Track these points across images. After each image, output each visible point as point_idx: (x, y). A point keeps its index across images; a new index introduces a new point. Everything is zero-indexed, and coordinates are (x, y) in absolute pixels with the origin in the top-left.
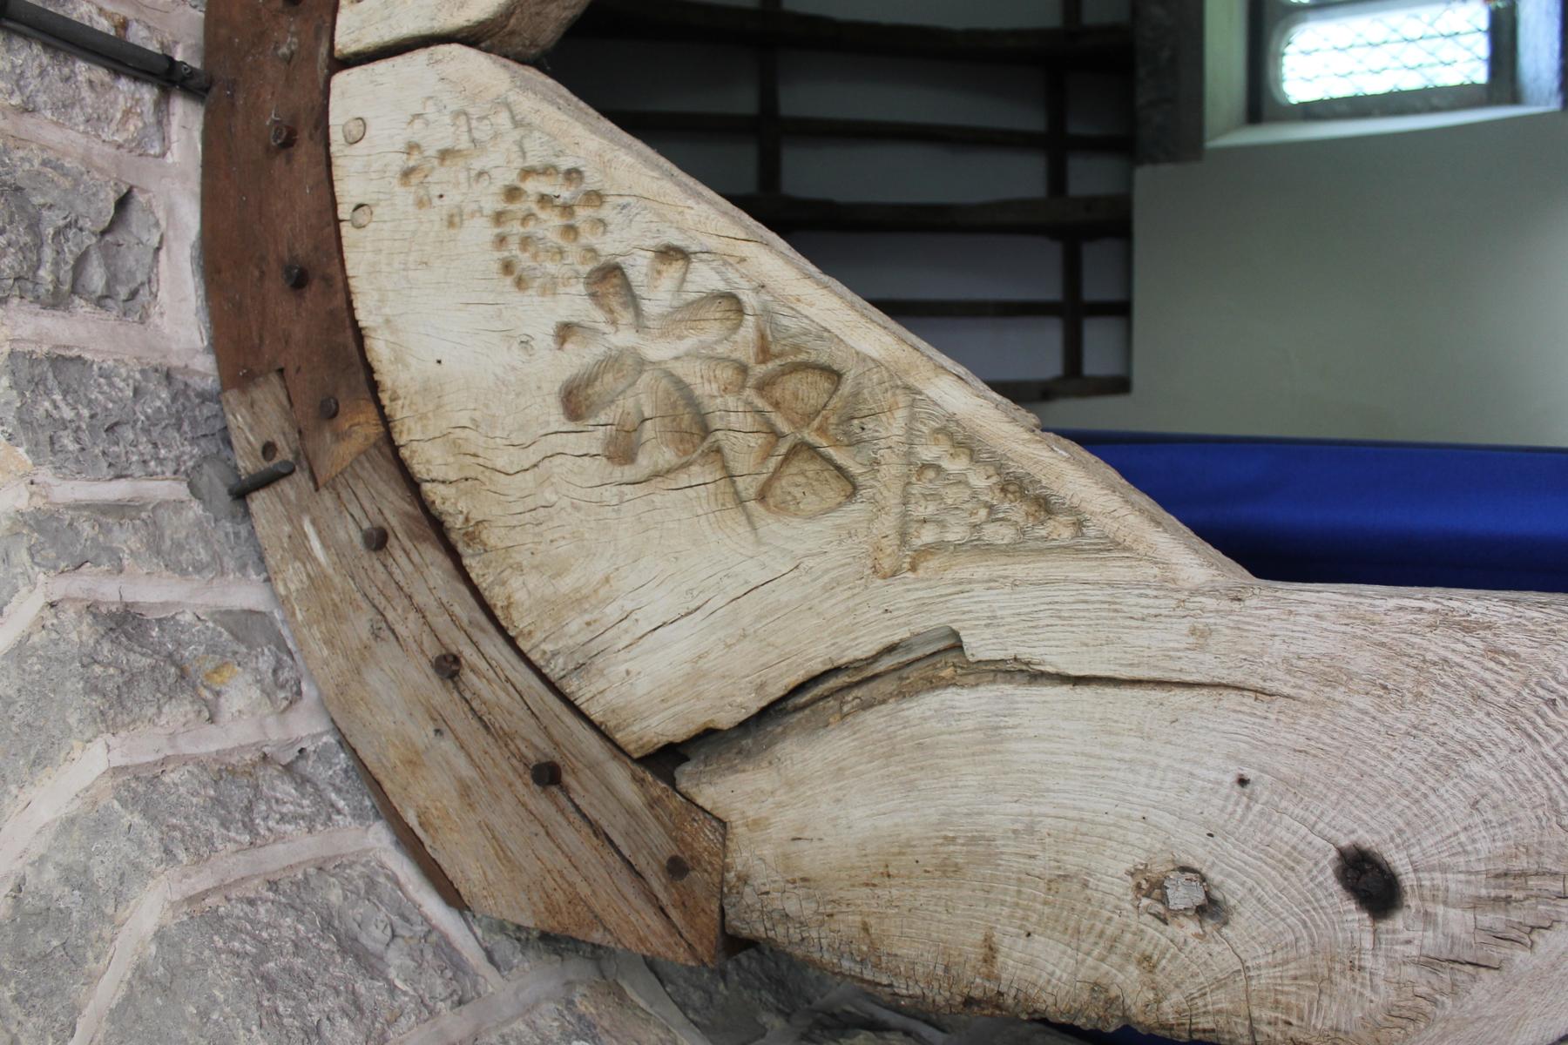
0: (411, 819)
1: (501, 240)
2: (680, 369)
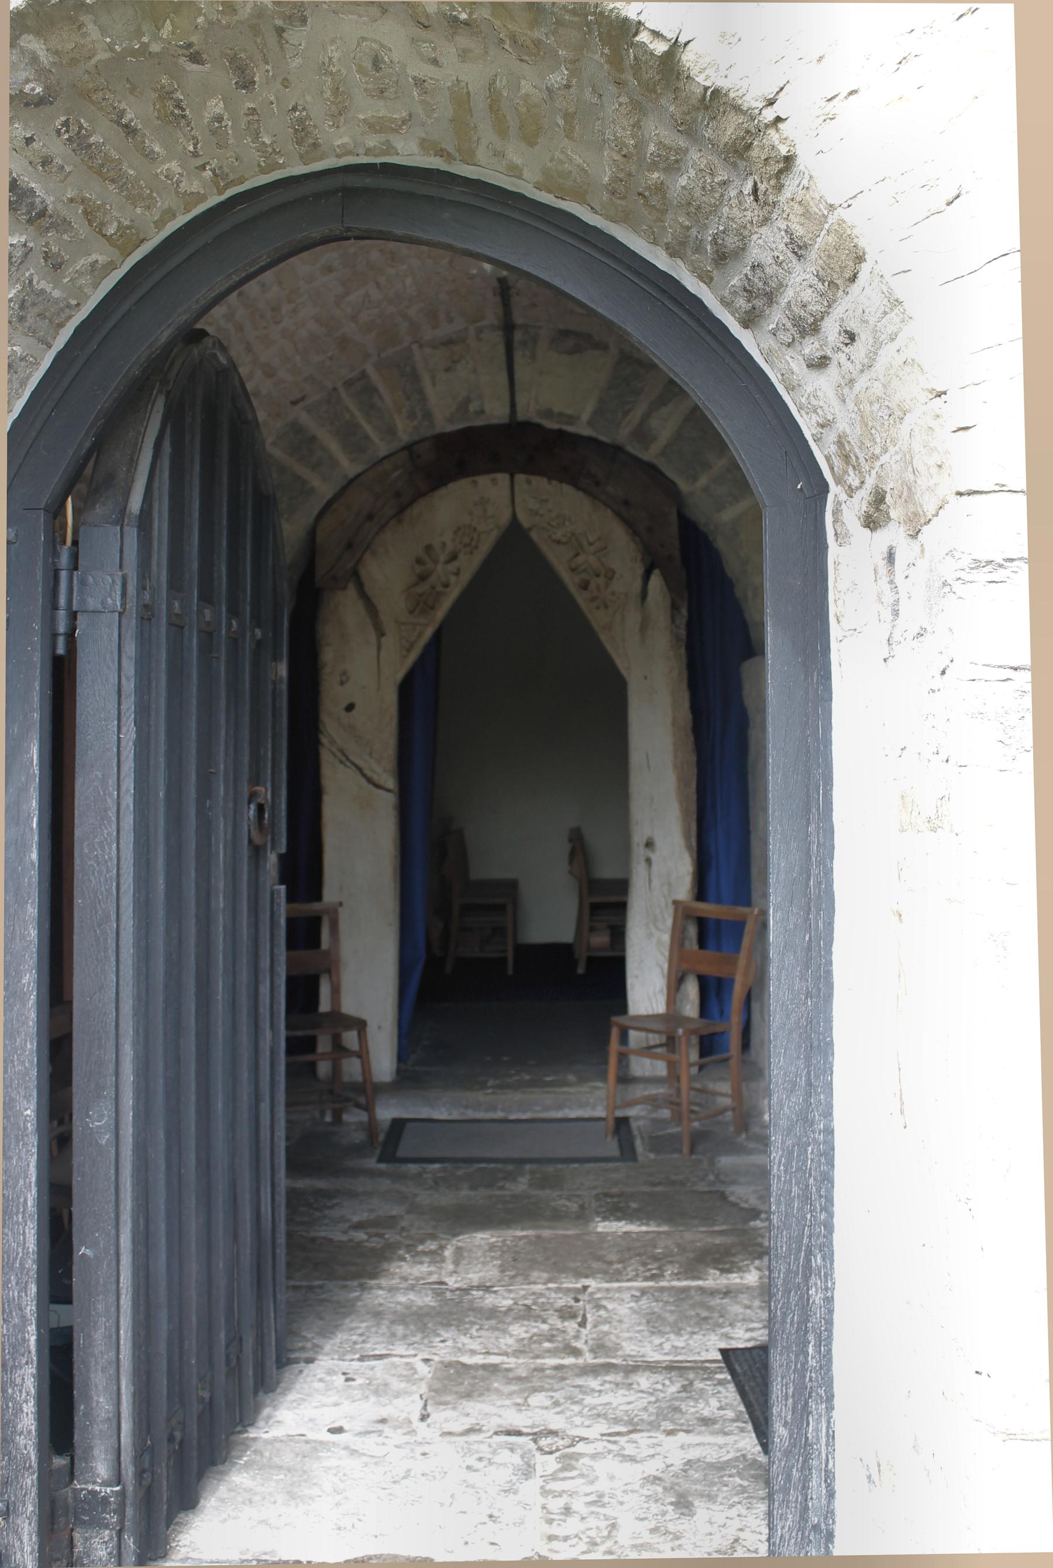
0: (335, 506)
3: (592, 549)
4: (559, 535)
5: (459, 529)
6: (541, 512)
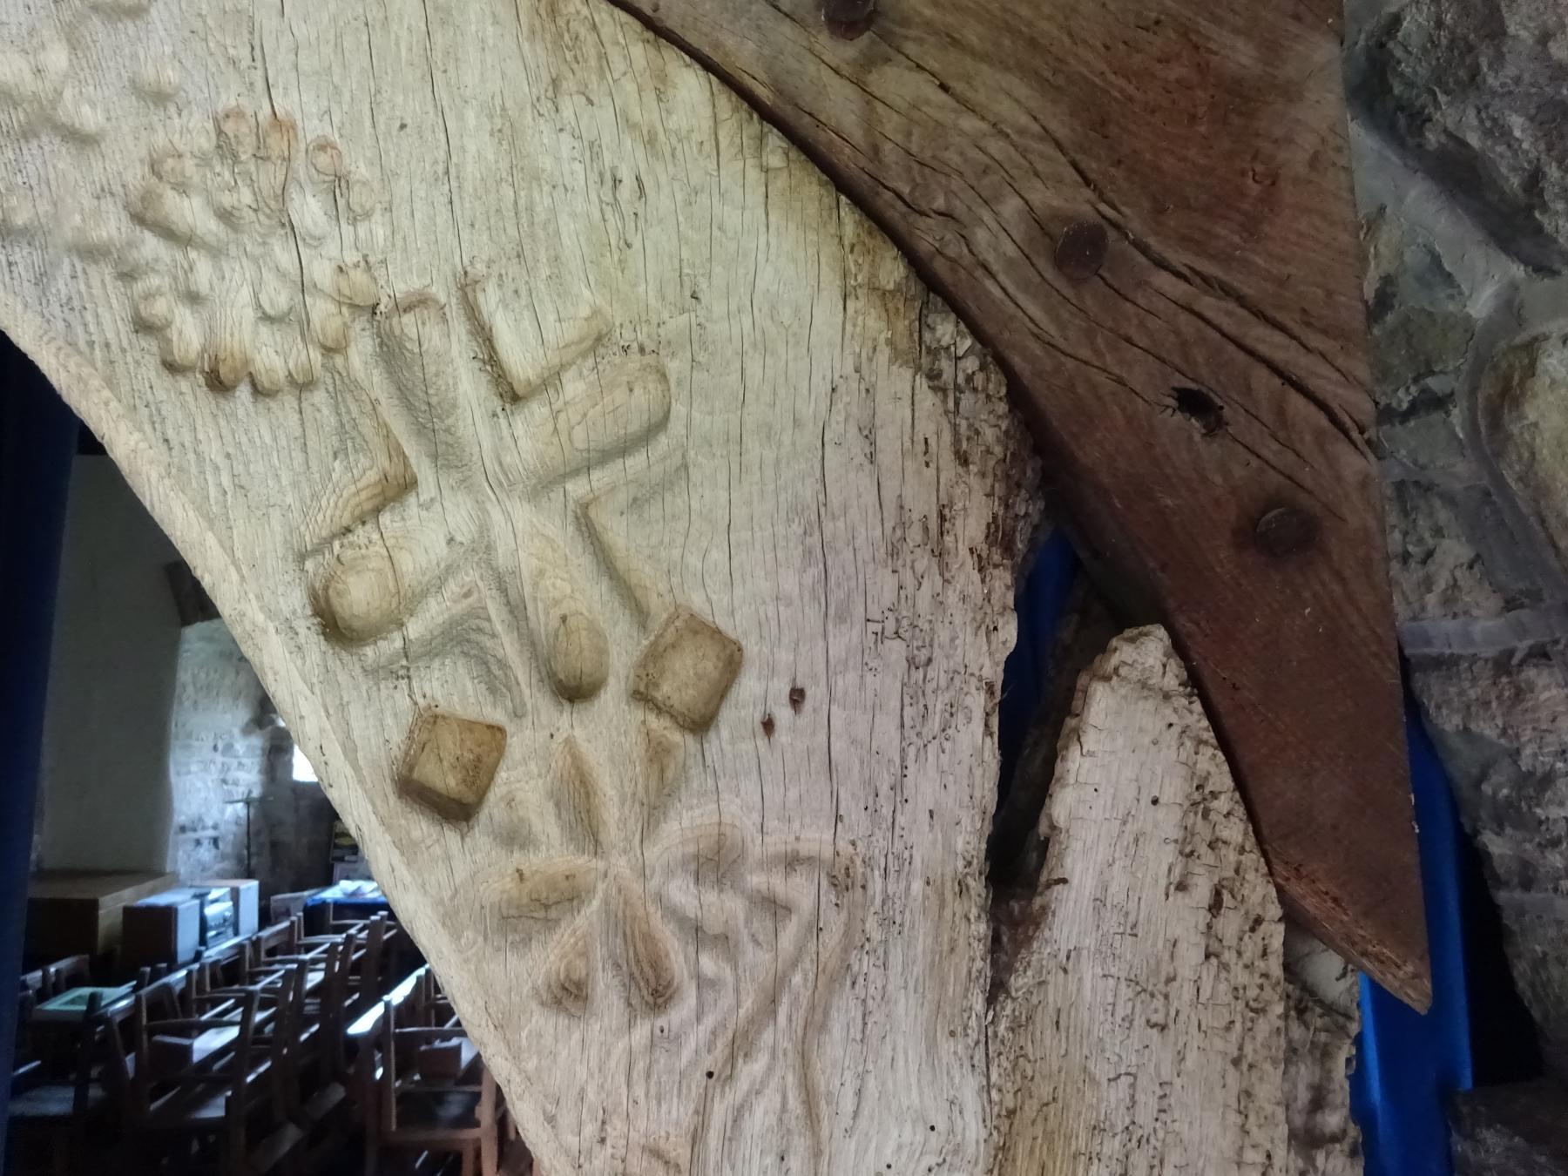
3: (528, 437)
4: (235, 306)
6: (89, 118)
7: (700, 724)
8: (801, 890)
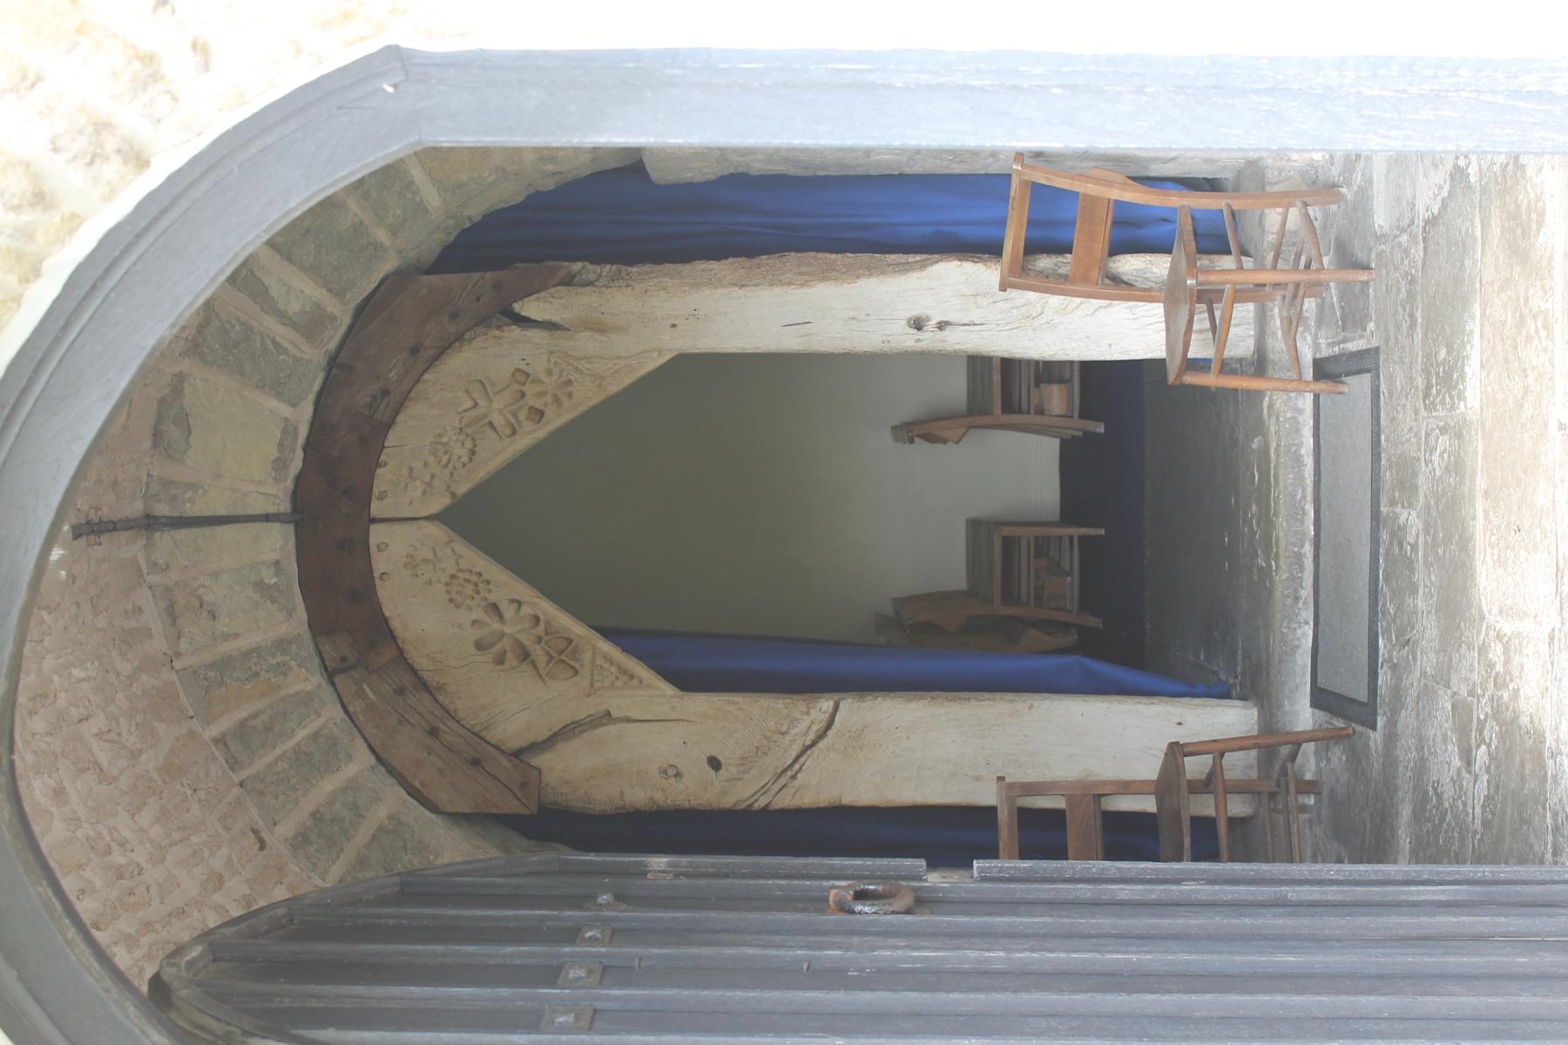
0: (417, 784)
1: (448, 592)
2: (519, 636)
3: (482, 403)
4: (461, 452)
5: (451, 601)
6: (428, 478)
7: (528, 375)
8: (553, 359)
